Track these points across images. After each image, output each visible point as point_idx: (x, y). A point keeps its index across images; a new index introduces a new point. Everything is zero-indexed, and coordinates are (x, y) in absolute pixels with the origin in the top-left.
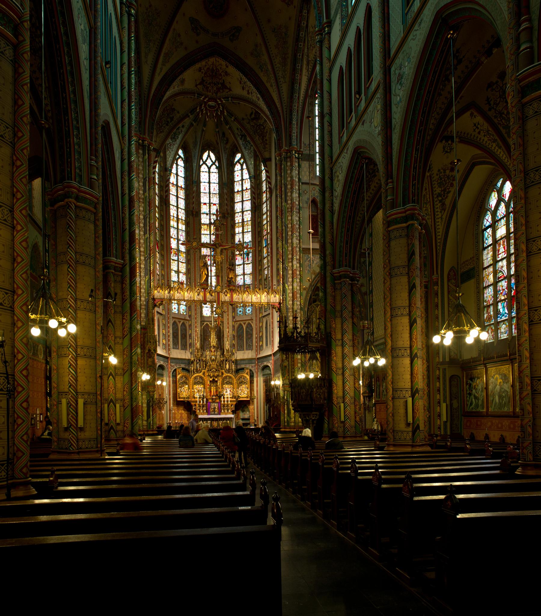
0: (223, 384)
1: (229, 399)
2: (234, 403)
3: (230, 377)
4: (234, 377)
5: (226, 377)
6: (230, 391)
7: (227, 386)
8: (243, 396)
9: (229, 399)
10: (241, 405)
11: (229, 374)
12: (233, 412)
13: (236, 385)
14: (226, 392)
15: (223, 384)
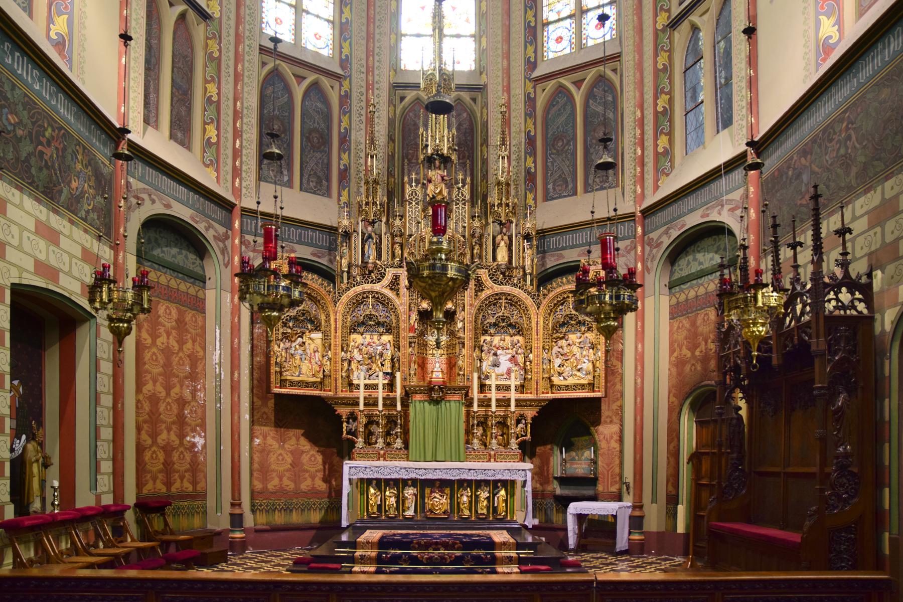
0: (481, 329)
1: (513, 395)
2: (530, 413)
3: (513, 302)
4: (529, 301)
5: (494, 301)
6: (513, 359)
7: (496, 340)
8: (571, 381)
9: (513, 395)
10: (563, 422)
11: (507, 289)
12: (527, 451)
13: (537, 340)
14: (496, 365)
15: (481, 329)
